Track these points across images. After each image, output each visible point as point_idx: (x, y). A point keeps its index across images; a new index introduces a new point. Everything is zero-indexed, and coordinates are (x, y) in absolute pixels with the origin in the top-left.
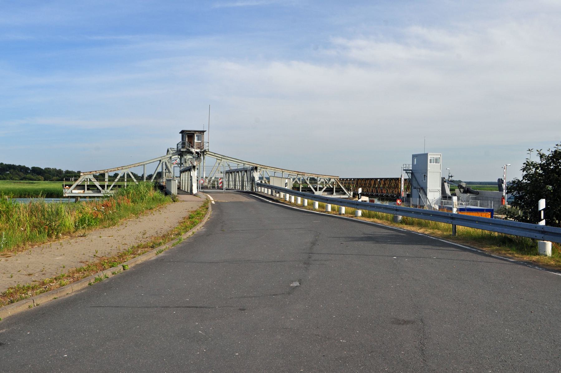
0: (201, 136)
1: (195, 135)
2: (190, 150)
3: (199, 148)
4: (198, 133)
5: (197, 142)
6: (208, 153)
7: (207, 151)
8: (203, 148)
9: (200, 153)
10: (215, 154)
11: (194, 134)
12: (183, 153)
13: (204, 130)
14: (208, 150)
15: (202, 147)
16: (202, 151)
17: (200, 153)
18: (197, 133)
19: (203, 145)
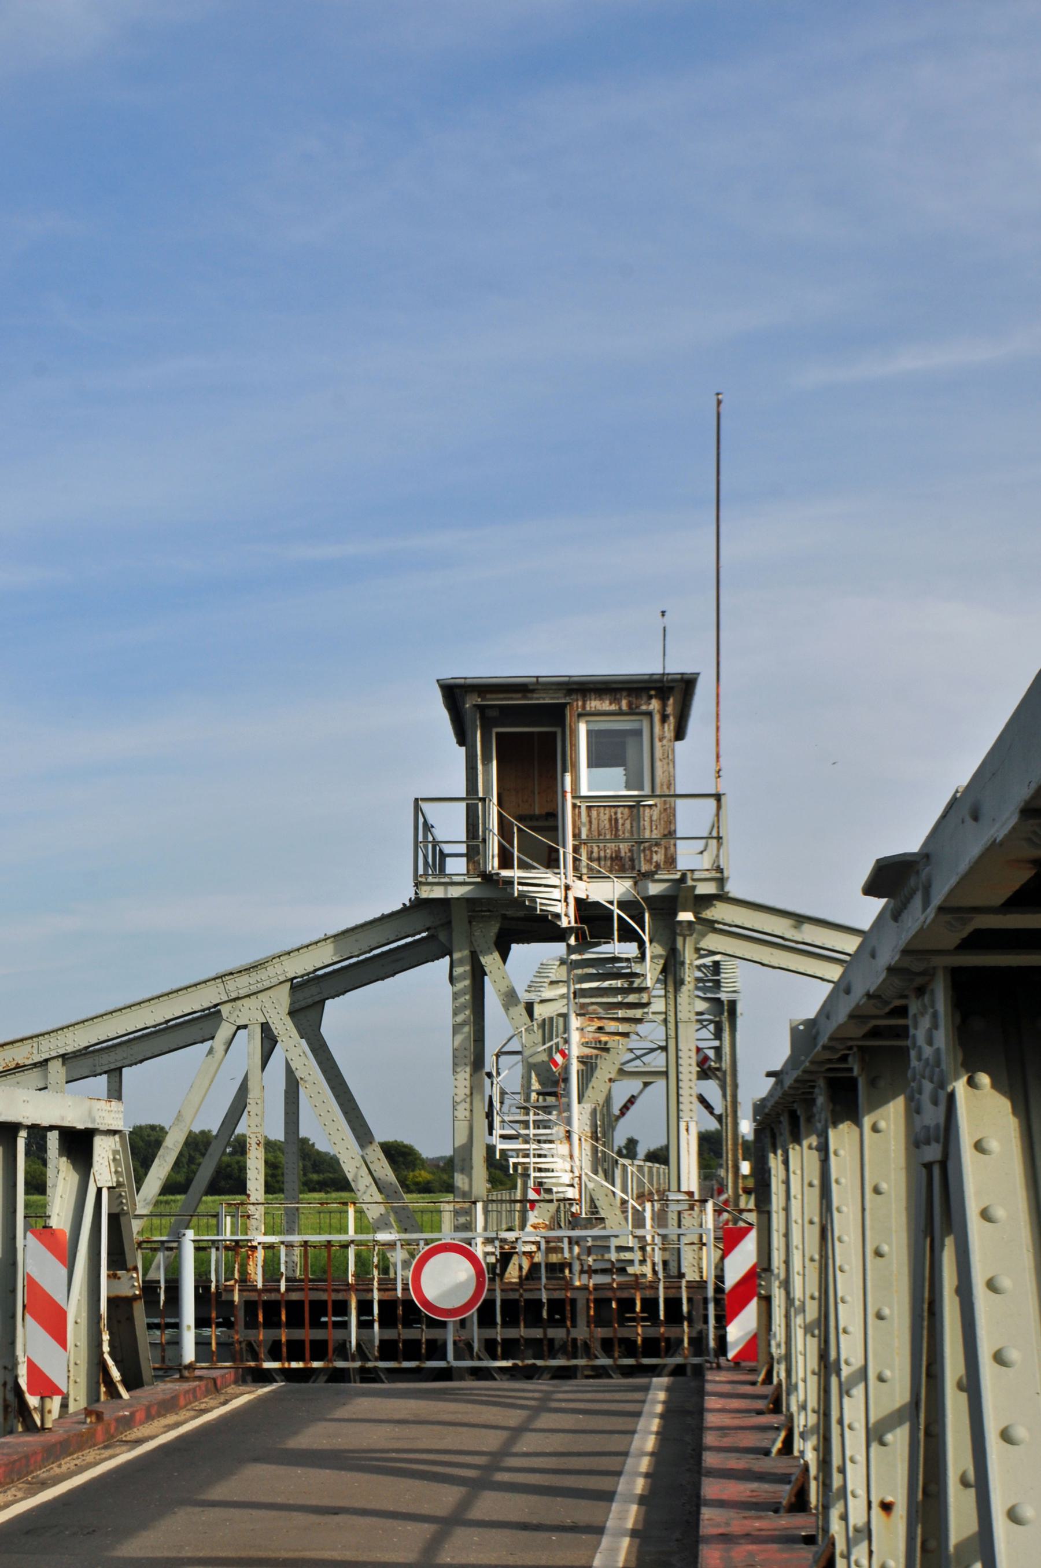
0: (638, 733)
1: (583, 728)
2: (509, 882)
3: (620, 865)
4: (605, 705)
5: (594, 803)
6: (719, 912)
7: (704, 889)
8: (671, 861)
9: (617, 911)
10: (800, 919)
11: (556, 715)
12: (448, 924)
13: (676, 666)
14: (721, 881)
15: (658, 857)
16: (654, 889)
17: (617, 911)
18: (595, 704)
19: (670, 835)
